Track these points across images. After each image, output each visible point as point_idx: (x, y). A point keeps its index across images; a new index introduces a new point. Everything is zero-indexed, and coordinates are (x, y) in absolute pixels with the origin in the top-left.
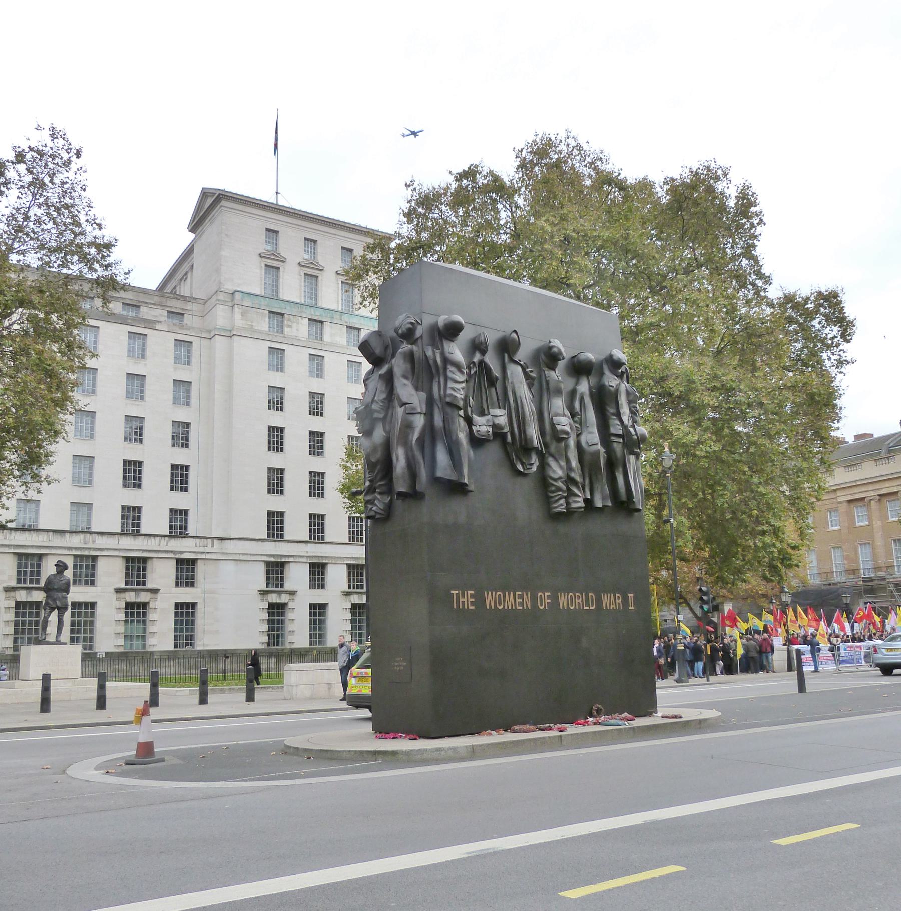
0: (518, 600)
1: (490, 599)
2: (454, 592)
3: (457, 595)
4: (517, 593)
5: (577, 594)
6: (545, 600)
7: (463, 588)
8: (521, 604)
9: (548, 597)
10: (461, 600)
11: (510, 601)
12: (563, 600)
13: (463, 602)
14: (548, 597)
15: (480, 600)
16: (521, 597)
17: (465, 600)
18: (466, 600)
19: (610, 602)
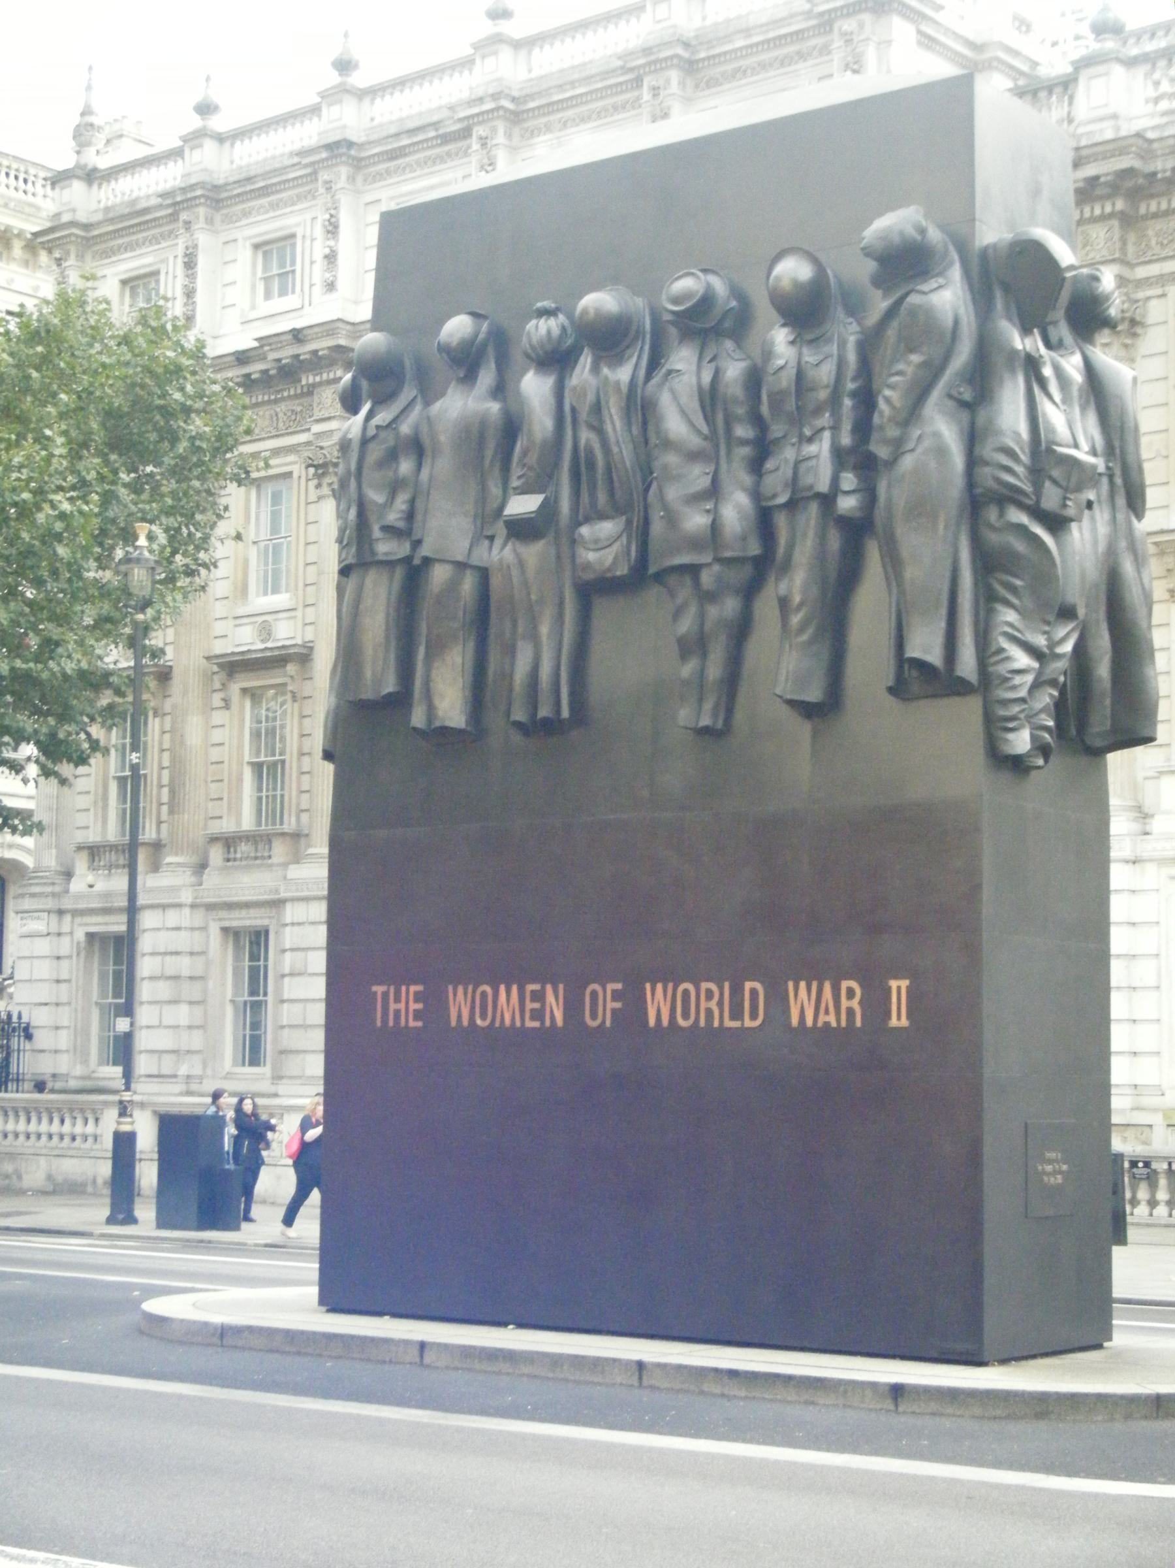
0: (530, 1005)
1: (460, 1005)
2: (379, 989)
3: (385, 995)
4: (531, 987)
5: (704, 986)
6: (605, 1002)
7: (400, 979)
8: (538, 1015)
9: (616, 996)
10: (393, 1006)
11: (508, 1006)
12: (658, 1004)
13: (397, 1013)
14: (616, 996)
16: (539, 996)
17: (402, 1006)
19: (805, 1004)
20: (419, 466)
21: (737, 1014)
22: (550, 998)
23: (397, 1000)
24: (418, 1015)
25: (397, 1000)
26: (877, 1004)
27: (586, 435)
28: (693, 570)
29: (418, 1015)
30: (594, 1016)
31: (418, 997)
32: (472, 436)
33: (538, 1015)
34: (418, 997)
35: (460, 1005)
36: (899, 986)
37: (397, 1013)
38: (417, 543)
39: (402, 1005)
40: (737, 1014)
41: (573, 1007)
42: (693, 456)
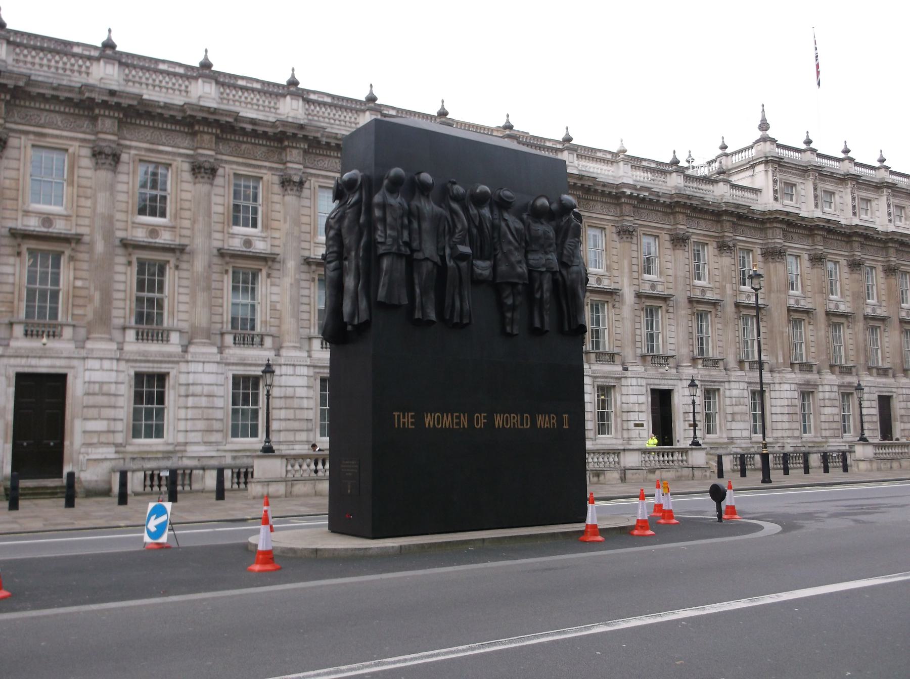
1: (429, 420)
2: (396, 414)
3: (399, 416)
6: (481, 420)
11: (447, 421)
12: (499, 421)
13: (404, 423)
15: (419, 420)
16: (458, 417)
18: (407, 420)
19: (543, 422)
20: (410, 222)
21: (522, 424)
22: (462, 418)
23: (404, 417)
24: (412, 423)
25: (404, 417)
26: (560, 422)
27: (475, 231)
28: (514, 285)
29: (412, 423)
30: (478, 424)
31: (412, 417)
32: (437, 220)
33: (458, 424)
34: (412, 417)
35: (429, 420)
36: (566, 416)
37: (404, 423)
38: (413, 251)
39: (407, 420)
40: (522, 424)
41: (471, 421)
42: (516, 249)
